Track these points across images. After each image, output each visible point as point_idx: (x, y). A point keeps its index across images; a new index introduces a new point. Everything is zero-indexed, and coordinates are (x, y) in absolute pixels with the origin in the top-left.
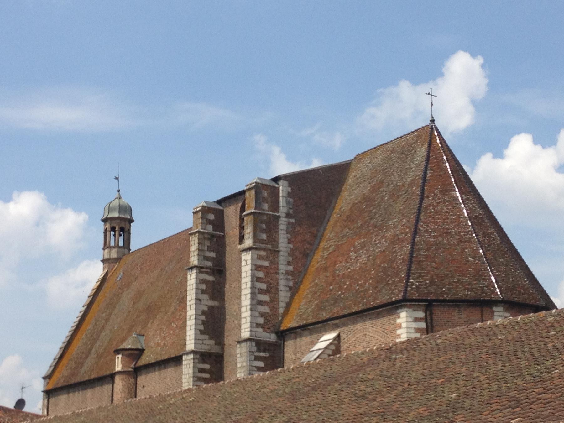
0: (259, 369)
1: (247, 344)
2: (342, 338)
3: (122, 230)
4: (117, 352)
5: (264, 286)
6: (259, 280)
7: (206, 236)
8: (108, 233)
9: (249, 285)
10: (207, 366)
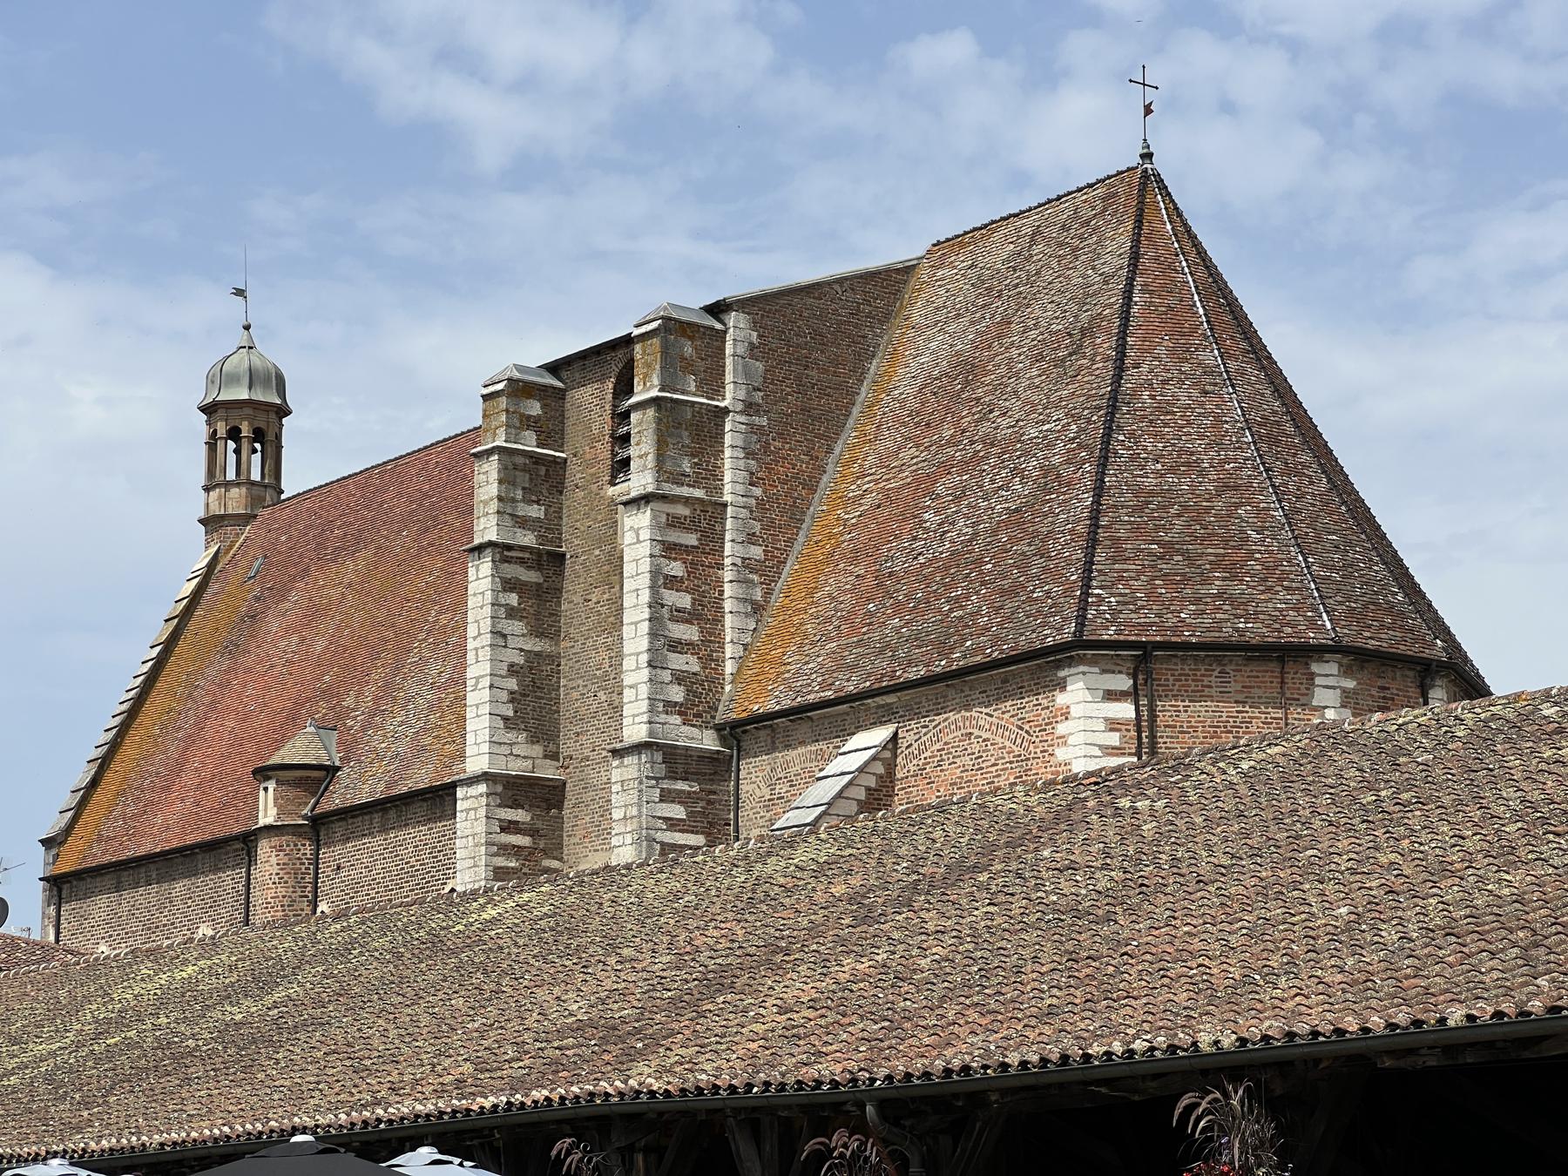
0: (672, 824)
1: (640, 759)
2: (903, 744)
3: (259, 435)
4: (263, 773)
5: (685, 601)
6: (672, 582)
7: (520, 460)
8: (220, 444)
9: (645, 596)
10: (520, 815)
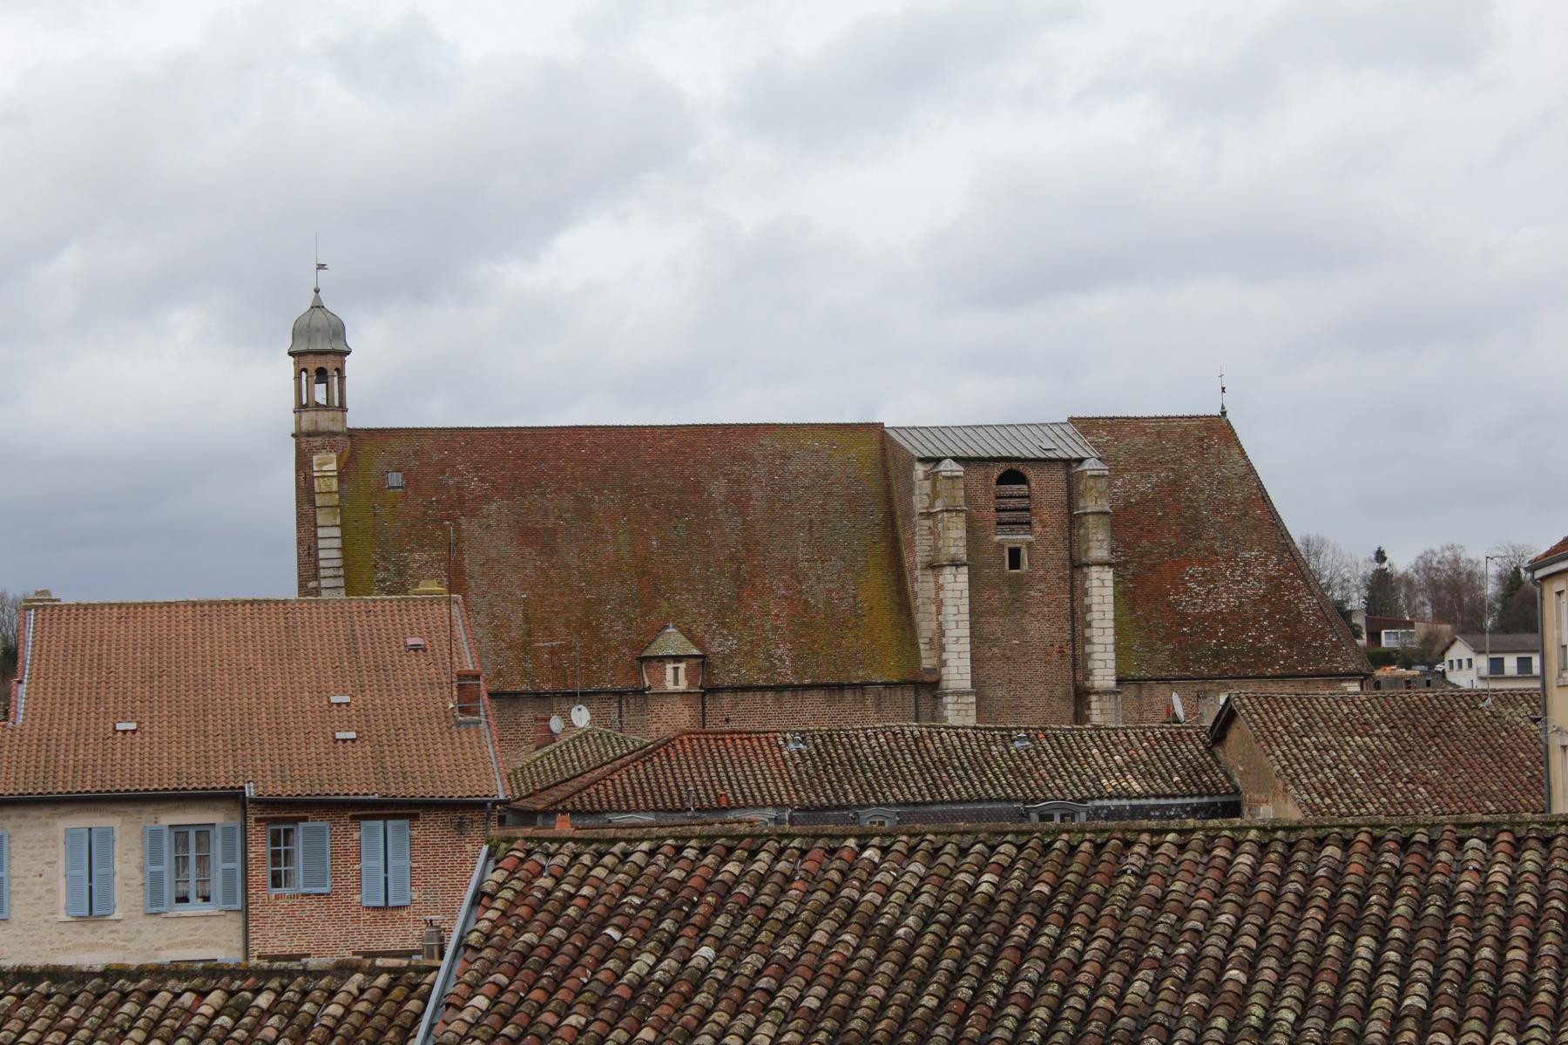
1: (1116, 699)
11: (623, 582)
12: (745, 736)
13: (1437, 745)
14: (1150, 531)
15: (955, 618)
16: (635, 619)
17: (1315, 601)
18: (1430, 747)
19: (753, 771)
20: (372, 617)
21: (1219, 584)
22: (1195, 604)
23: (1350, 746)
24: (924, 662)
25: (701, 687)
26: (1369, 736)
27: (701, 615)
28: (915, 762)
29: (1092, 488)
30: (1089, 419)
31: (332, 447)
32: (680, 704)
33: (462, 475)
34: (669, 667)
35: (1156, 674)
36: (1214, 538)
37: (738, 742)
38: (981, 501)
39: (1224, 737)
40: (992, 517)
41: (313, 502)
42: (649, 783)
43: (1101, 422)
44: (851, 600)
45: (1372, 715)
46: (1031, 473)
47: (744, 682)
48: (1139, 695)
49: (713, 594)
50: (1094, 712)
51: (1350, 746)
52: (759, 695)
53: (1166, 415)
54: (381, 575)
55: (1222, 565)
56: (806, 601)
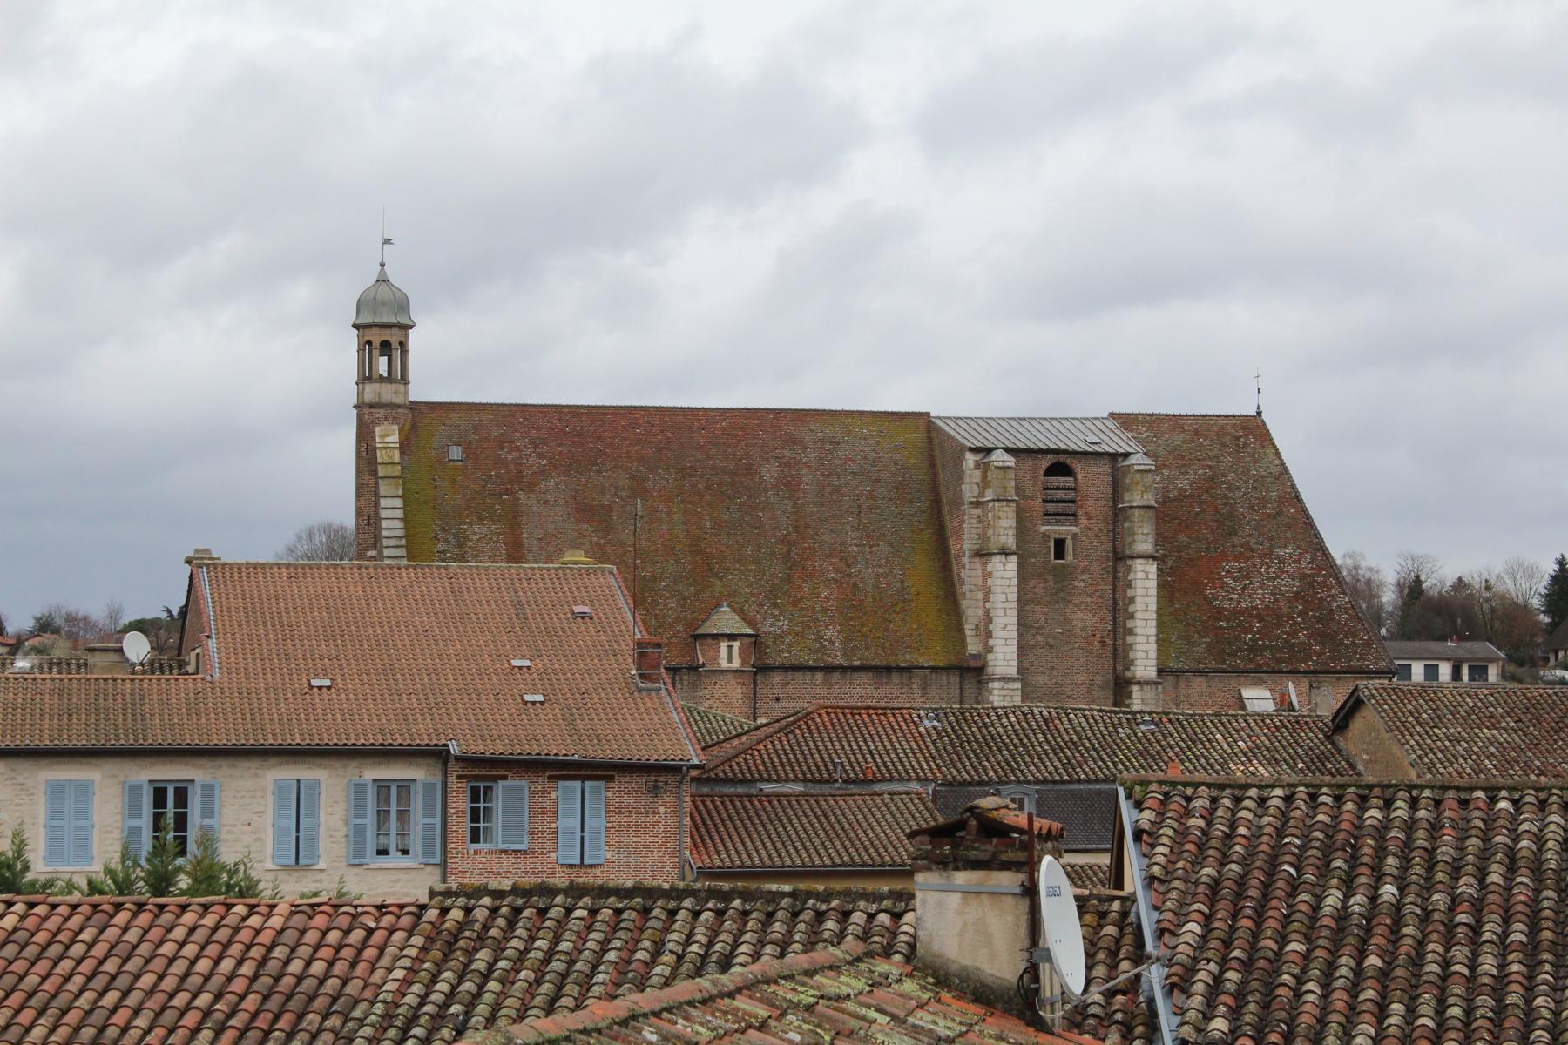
1: (1157, 689)
11: (678, 561)
12: (880, 711)
13: (1562, 739)
14: (1187, 526)
15: (1004, 605)
16: (689, 598)
17: (1347, 600)
18: (1555, 741)
19: (892, 745)
20: (533, 585)
21: (1255, 580)
22: (1231, 599)
23: (1479, 738)
24: (969, 647)
25: (753, 666)
26: (1497, 729)
27: (753, 595)
28: (1048, 742)
29: (1138, 483)
30: (1129, 414)
31: (395, 419)
32: (733, 682)
33: (520, 451)
34: (724, 645)
35: (1193, 666)
36: (1250, 535)
37: (874, 717)
38: (1029, 492)
39: (1347, 726)
40: (1038, 506)
41: (375, 473)
42: (795, 755)
43: (1140, 418)
44: (899, 585)
45: (1496, 709)
46: (1077, 466)
47: (794, 662)
48: (1176, 686)
49: (765, 575)
50: (1135, 701)
51: (1479, 738)
52: (808, 675)
53: (1203, 413)
54: (441, 546)
55: (1258, 562)
56: (855, 585)
